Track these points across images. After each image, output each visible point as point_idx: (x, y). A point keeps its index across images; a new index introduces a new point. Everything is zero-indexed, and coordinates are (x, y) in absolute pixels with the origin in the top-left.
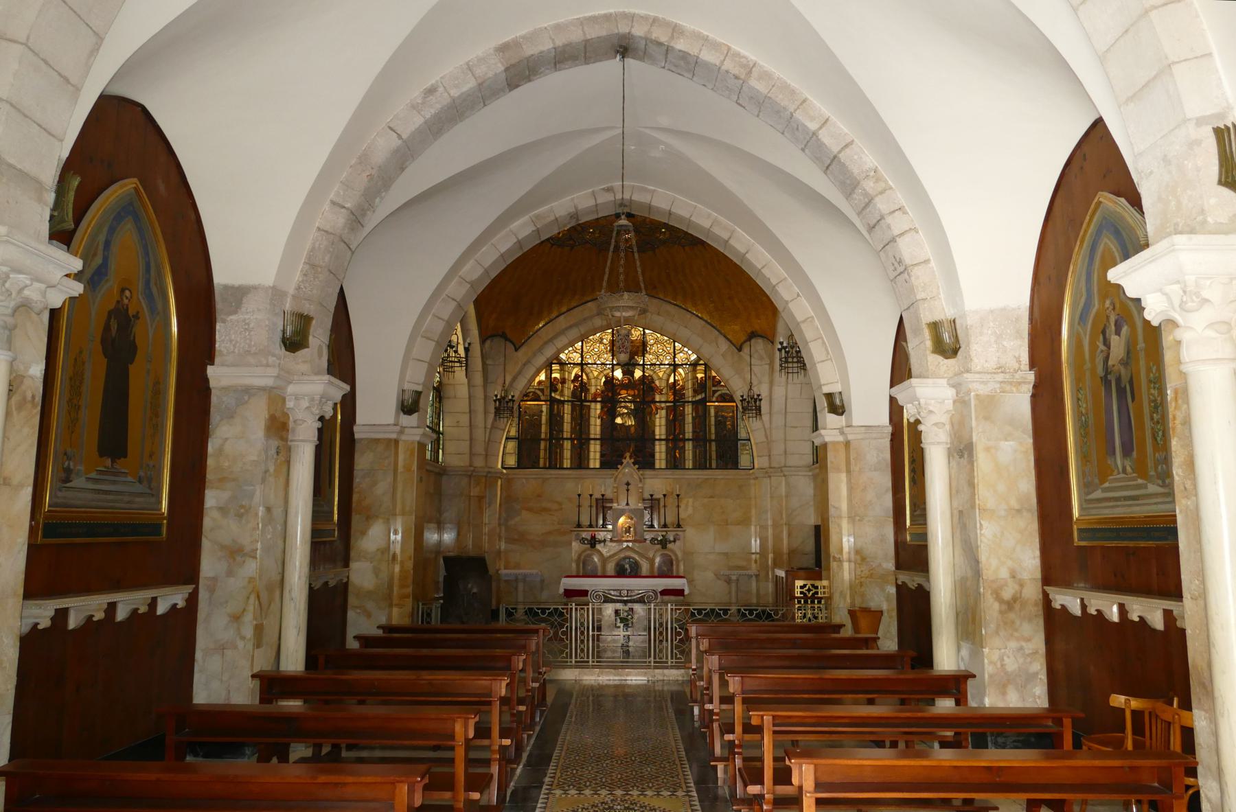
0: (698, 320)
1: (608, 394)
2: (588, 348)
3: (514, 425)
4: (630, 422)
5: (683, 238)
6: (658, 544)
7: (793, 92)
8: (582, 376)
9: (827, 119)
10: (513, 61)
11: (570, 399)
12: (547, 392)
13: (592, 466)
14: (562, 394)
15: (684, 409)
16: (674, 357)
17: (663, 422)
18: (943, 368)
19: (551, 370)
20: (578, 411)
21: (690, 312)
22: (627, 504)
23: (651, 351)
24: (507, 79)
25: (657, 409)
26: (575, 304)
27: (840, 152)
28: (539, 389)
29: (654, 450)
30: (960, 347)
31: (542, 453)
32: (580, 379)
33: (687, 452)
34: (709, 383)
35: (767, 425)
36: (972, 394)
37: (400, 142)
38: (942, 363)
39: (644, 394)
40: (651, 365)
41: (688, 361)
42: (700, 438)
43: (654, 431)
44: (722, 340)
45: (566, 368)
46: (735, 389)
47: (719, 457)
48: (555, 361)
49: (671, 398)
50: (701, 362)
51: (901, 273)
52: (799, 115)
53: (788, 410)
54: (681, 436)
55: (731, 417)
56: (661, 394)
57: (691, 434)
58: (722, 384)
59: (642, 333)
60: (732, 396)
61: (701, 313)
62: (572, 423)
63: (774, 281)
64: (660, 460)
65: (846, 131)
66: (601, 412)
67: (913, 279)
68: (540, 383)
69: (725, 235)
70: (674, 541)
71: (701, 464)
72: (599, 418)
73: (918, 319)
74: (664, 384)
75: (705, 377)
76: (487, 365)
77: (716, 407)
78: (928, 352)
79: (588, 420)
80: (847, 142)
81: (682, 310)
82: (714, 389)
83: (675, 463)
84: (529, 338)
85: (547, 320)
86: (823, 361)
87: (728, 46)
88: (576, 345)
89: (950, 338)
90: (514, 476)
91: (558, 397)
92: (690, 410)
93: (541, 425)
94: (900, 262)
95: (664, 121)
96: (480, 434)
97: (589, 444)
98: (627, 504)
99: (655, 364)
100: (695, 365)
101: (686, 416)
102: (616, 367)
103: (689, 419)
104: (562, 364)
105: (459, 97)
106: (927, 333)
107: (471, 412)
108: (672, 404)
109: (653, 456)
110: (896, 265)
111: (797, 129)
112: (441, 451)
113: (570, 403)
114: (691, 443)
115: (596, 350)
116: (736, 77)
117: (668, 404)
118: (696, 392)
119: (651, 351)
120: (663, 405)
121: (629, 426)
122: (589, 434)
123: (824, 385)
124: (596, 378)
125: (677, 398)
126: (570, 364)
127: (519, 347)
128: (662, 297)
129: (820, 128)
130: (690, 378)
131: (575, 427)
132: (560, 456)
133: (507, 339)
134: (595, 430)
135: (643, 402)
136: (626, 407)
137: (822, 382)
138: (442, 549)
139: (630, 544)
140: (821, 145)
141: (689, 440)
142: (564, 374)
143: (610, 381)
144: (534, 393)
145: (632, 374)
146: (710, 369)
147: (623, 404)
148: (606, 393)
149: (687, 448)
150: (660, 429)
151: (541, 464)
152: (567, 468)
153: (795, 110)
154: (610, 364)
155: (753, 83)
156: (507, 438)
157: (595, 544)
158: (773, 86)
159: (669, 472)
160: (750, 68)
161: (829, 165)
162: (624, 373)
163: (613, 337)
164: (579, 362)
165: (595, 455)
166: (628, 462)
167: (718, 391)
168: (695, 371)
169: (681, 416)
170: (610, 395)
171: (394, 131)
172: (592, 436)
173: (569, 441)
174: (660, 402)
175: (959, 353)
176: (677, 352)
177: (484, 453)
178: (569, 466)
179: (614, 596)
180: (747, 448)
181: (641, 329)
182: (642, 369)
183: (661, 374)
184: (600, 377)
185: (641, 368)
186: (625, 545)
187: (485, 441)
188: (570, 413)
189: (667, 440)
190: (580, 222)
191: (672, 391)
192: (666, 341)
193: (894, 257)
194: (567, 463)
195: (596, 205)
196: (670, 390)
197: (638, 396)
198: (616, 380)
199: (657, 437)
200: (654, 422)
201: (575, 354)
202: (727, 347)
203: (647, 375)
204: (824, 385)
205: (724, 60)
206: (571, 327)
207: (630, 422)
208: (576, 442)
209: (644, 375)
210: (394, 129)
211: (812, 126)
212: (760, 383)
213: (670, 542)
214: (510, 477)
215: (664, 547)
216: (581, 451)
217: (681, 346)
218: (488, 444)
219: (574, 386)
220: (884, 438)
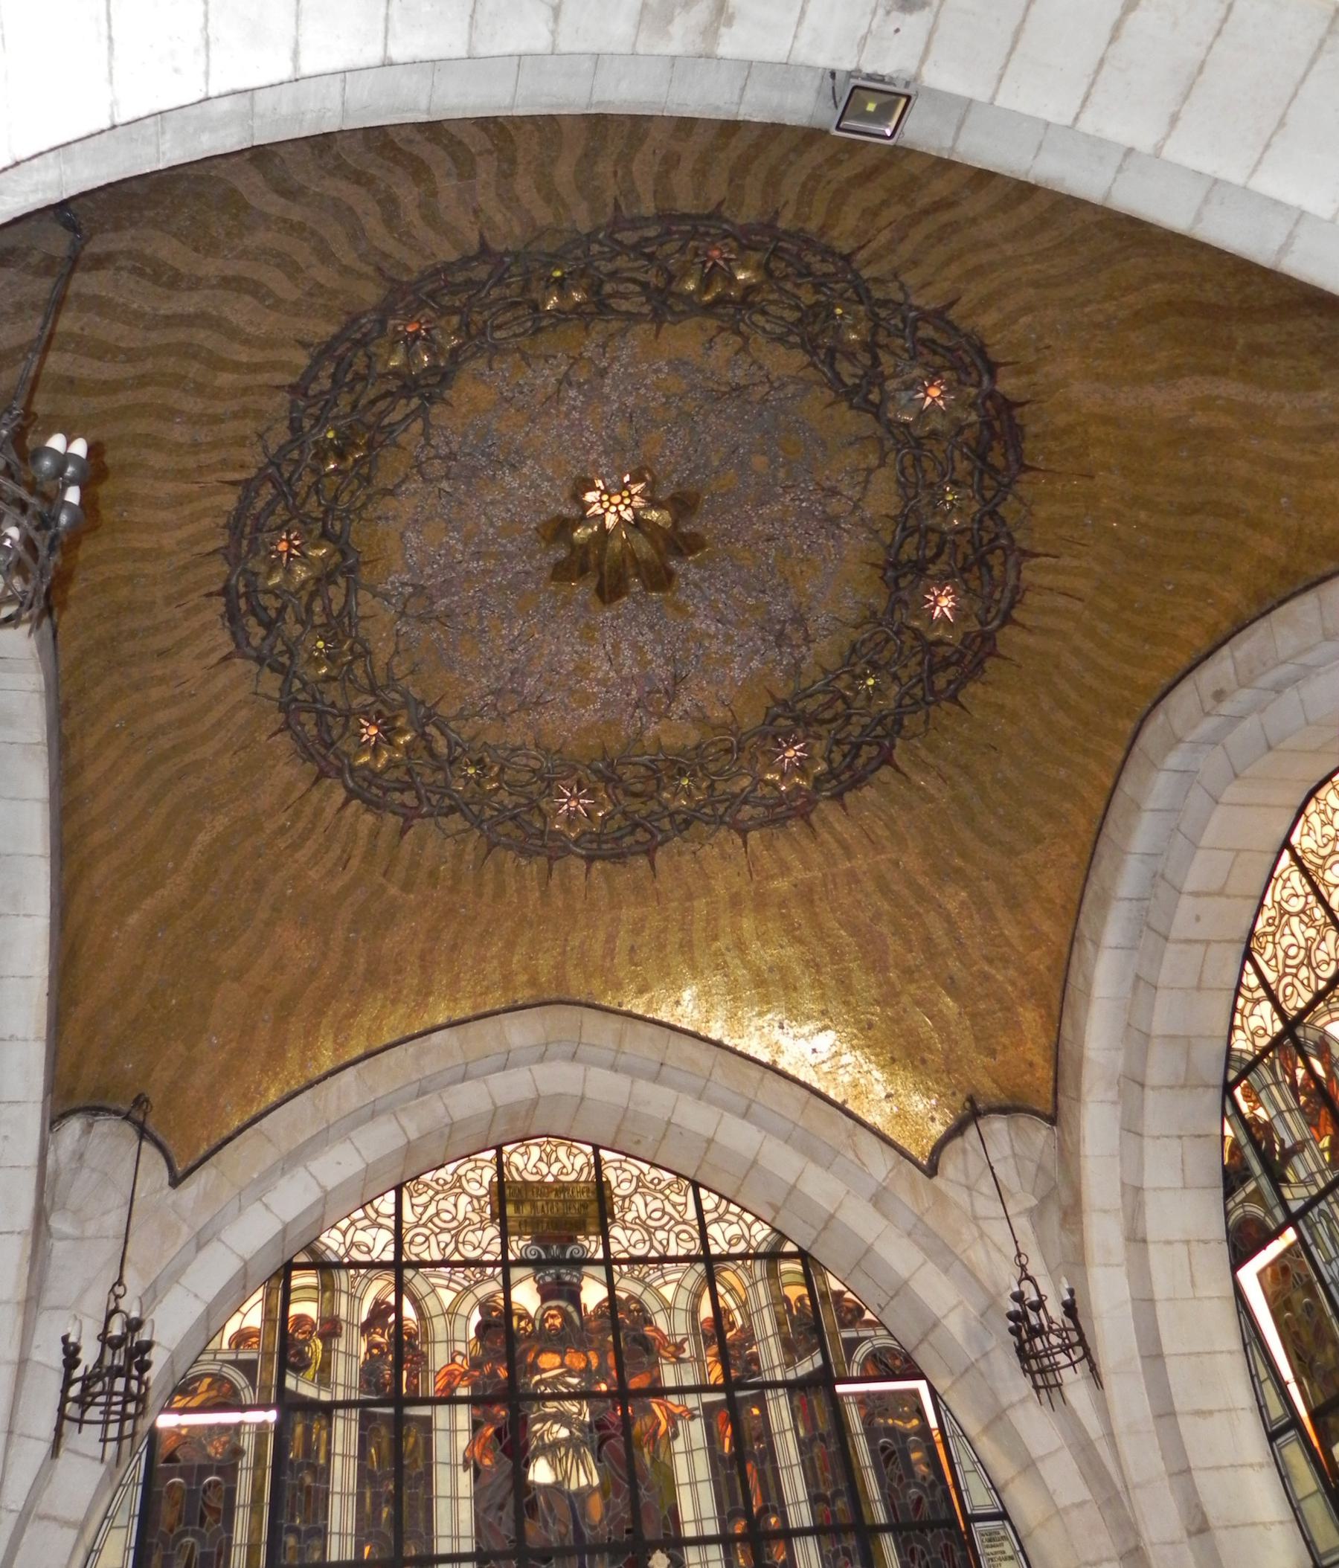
0: (783, 1082)
1: (494, 1373)
2: (419, 1210)
4: (585, 1476)
5: (745, 802)
8: (398, 1308)
11: (355, 1396)
15: (764, 1410)
16: (704, 1236)
20: (385, 1445)
23: (629, 1217)
25: (672, 1419)
32: (392, 1318)
34: (828, 1318)
35: (1093, 1425)
39: (620, 1366)
40: (633, 1261)
41: (748, 1243)
45: (343, 1278)
49: (716, 1375)
53: (1168, 1346)
54: (773, 1520)
56: (680, 1361)
58: (868, 1316)
59: (592, 1160)
60: (908, 1359)
66: (473, 1442)
72: (466, 1462)
74: (681, 1325)
77: (863, 1399)
79: (427, 1477)
82: (847, 1334)
88: (376, 1203)
91: (308, 1391)
99: (644, 1260)
100: (773, 1256)
101: (777, 1440)
102: (516, 1273)
103: (788, 1449)
104: (324, 1267)
108: (720, 1397)
113: (355, 1413)
114: (811, 1542)
117: (709, 1398)
118: (792, 1350)
119: (629, 1217)
120: (692, 1401)
121: (582, 1494)
124: (451, 1313)
125: (733, 1373)
126: (356, 1265)
130: (764, 1303)
134: (455, 1514)
135: (622, 1395)
136: (561, 1418)
141: (803, 1532)
147: (551, 1407)
148: (487, 1369)
154: (493, 1264)
163: (500, 1172)
164: (389, 1256)
167: (858, 1341)
168: (773, 1275)
169: (759, 1439)
170: (503, 1373)
174: (681, 1390)
176: (708, 1218)
181: (589, 1149)
182: (604, 1278)
183: (668, 1292)
184: (464, 1309)
185: (600, 1272)
188: (354, 1450)
189: (724, 1539)
191: (715, 1349)
192: (669, 1185)
196: (707, 1347)
198: (521, 1318)
199: (689, 1531)
201: (373, 1231)
202: (890, 1165)
203: (623, 1295)
206: (372, 1113)
207: (585, 1476)
209: (612, 1297)
217: (716, 1198)
219: (371, 1346)
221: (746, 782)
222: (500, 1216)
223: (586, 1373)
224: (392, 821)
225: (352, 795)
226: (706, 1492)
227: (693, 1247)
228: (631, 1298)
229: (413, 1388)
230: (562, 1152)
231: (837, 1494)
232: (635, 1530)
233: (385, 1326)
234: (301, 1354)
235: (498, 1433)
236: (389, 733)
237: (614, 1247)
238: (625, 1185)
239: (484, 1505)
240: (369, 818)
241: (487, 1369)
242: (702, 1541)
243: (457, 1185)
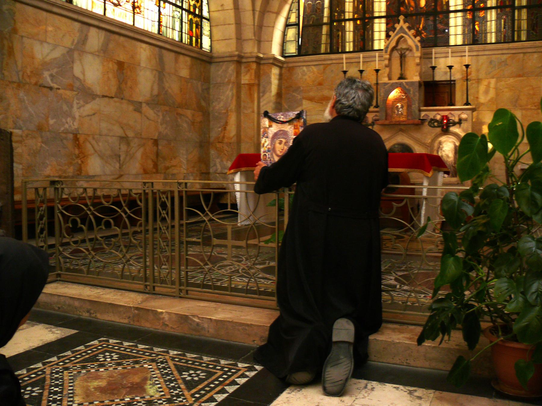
3: (294, 11)
6: (438, 127)
22: (402, 77)
33: (489, 23)
54: (482, 5)
93: (323, 8)
96: (248, 18)
97: (373, 24)
114: (494, 11)
122: (373, 12)
131: (358, 6)
132: (342, 42)
138: (212, 140)
141: (491, 8)
149: (489, 18)
156: (287, 25)
166: (401, 27)
172: (376, 14)
173: (352, 22)
178: (351, 50)
187: (254, 25)
194: (349, 47)
199: (452, 9)
208: (358, 22)
214: (291, 65)
216: (364, 33)
239: (388, 3)
242: (456, 11)
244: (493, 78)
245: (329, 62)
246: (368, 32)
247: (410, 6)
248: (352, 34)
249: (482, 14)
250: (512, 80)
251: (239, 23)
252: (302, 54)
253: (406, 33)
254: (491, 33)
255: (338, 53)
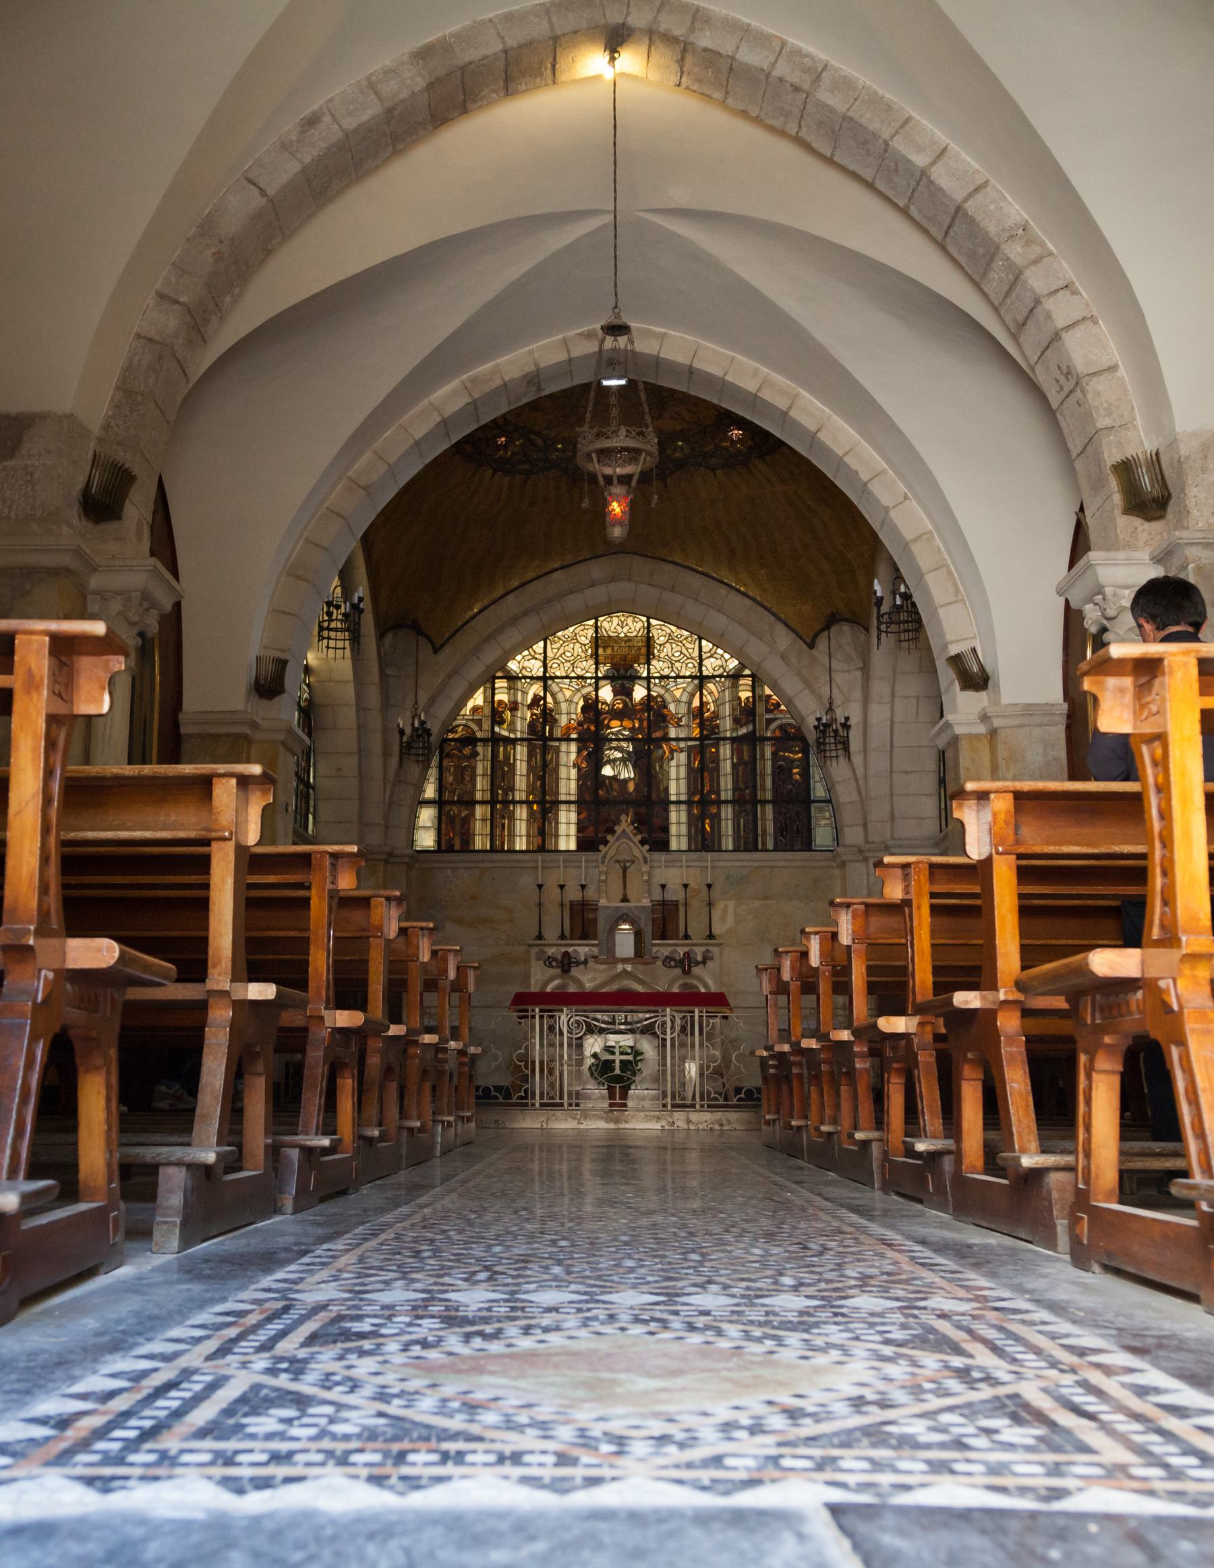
0: (739, 598)
1: (589, 728)
3: (432, 780)
4: (627, 773)
6: (676, 967)
7: (889, 108)
8: (545, 698)
9: (945, 149)
10: (441, 72)
11: (525, 736)
12: (487, 725)
13: (562, 847)
14: (512, 729)
15: (718, 751)
16: (701, 665)
17: (683, 772)
18: (1143, 537)
19: (493, 689)
21: (726, 584)
22: (625, 899)
24: (429, 105)
25: (672, 751)
26: (532, 575)
27: (966, 200)
28: (473, 720)
29: (667, 819)
30: (1170, 495)
31: (478, 825)
33: (723, 823)
34: (760, 708)
35: (860, 771)
36: (1191, 566)
37: (264, 201)
38: (1140, 529)
39: (649, 727)
40: (662, 678)
42: (746, 801)
43: (667, 789)
44: (781, 630)
45: (519, 685)
46: (804, 713)
47: (781, 830)
48: (499, 674)
49: (696, 733)
50: (747, 672)
51: (1071, 392)
52: (898, 144)
55: (799, 760)
56: (680, 726)
57: (730, 793)
61: (745, 585)
62: (528, 775)
63: (864, 476)
64: (678, 836)
65: (976, 166)
66: (578, 757)
67: (1090, 396)
68: (475, 709)
69: (781, 403)
70: (704, 962)
71: (748, 842)
72: (574, 766)
73: (1099, 461)
74: (683, 709)
75: (754, 696)
76: (388, 676)
78: (1118, 512)
79: (556, 770)
80: (978, 183)
81: (713, 582)
83: (703, 842)
84: (457, 631)
85: (486, 602)
86: (949, 604)
87: (780, 38)
89: (1152, 485)
90: (435, 865)
92: (728, 752)
94: (1068, 374)
95: (680, 197)
98: (625, 899)
99: (668, 677)
100: (735, 676)
101: (722, 763)
102: (602, 683)
103: (726, 767)
104: (512, 678)
105: (356, 130)
106: (1113, 484)
107: (362, 752)
109: (665, 829)
110: (1062, 379)
111: (896, 171)
112: (311, 817)
115: (568, 654)
116: (796, 89)
117: (690, 743)
118: (737, 722)
120: (682, 745)
121: (626, 781)
122: (557, 793)
123: (952, 642)
124: (569, 701)
126: (525, 677)
127: (441, 647)
128: (677, 559)
129: (933, 163)
132: (509, 835)
133: (420, 633)
134: (568, 787)
135: (649, 740)
137: (949, 638)
139: (629, 968)
140: (936, 192)
141: (726, 802)
142: (515, 695)
143: (592, 707)
144: (465, 726)
145: (629, 693)
146: (762, 683)
147: (614, 744)
148: (585, 726)
149: (723, 816)
150: (676, 783)
151: (478, 843)
152: (521, 851)
153: (893, 136)
154: (591, 678)
155: (824, 95)
157: (570, 967)
158: (855, 100)
159: (695, 855)
160: (817, 73)
161: (949, 227)
162: (616, 692)
163: (596, 632)
165: (568, 829)
166: (624, 831)
168: (735, 687)
169: (713, 762)
170: (593, 728)
171: (255, 184)
172: (563, 798)
173: (524, 806)
174: (677, 739)
175: (1170, 509)
177: (382, 822)
178: (524, 848)
179: (604, 1022)
180: (827, 815)
181: (644, 619)
183: (678, 694)
185: (644, 683)
186: (620, 967)
188: (525, 758)
189: (689, 803)
190: (544, 393)
193: (1059, 367)
194: (521, 844)
195: (570, 360)
197: (640, 729)
199: (673, 798)
200: (668, 773)
201: (533, 661)
203: (655, 694)
204: (952, 642)
205: (776, 61)
206: (526, 613)
207: (627, 773)
208: (535, 807)
209: (649, 695)
210: (256, 181)
211: (920, 160)
212: (847, 701)
213: (697, 964)
215: (687, 973)
217: (711, 645)
218: (390, 805)
219: (532, 714)
220: (1056, 724)
221: (711, 447)
222: (595, 655)
223: (632, 730)
224: (518, 478)
225: (495, 471)
226: (683, 783)
227: (695, 672)
228: (659, 696)
229: (551, 732)
230: (630, 619)
231: (746, 788)
232: (649, 796)
233: (539, 706)
234: (501, 717)
235: (589, 754)
236: (510, 440)
237: (652, 669)
238: (662, 639)
240: (507, 479)
241: (585, 726)
243: (575, 639)
244: (730, 899)
245: (490, 865)
246: (550, 823)
247: (613, 790)
248: (524, 824)
249: (714, 810)
250: (757, 903)
251: (362, 798)
252: (443, 848)
253: (630, 839)
254: (727, 836)
255: (503, 851)
